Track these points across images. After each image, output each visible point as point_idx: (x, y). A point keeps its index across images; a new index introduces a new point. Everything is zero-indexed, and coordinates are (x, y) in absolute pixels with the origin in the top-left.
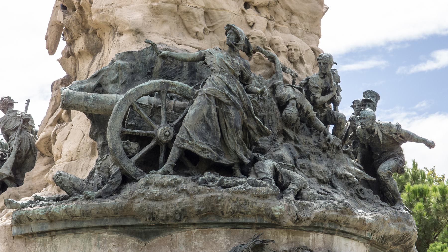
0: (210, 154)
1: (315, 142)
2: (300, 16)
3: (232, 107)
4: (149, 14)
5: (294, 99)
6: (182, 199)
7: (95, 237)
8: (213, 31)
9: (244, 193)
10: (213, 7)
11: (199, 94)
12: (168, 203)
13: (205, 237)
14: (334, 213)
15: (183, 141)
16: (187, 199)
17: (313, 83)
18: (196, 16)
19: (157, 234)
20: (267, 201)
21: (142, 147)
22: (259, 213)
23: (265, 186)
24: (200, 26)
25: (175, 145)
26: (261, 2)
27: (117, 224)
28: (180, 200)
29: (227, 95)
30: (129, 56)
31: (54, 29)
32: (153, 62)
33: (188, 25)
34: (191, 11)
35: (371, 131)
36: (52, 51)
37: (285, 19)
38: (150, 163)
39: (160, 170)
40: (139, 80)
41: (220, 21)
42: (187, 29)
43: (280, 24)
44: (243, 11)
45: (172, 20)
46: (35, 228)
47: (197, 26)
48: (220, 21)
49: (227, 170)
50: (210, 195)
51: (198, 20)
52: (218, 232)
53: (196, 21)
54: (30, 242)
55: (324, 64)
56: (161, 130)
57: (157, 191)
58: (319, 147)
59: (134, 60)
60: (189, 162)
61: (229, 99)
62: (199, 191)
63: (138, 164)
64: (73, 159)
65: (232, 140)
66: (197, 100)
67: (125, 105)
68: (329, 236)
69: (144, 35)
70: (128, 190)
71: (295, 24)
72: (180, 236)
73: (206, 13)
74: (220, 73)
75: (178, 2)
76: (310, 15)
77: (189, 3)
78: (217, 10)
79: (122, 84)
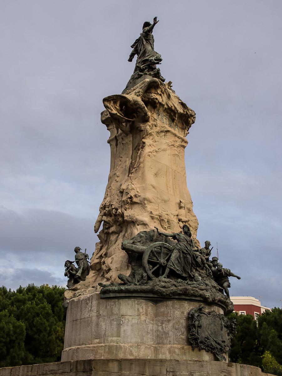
0: (180, 272)
1: (205, 273)
2: (193, 228)
3: (188, 255)
5: (200, 256)
6: (173, 288)
7: (137, 300)
9: (196, 288)
10: (170, 219)
11: (175, 249)
12: (168, 289)
13: (180, 304)
14: (222, 299)
15: (171, 266)
16: (175, 288)
17: (203, 251)
19: (161, 301)
20: (203, 292)
21: (153, 267)
22: (201, 296)
23: (203, 286)
25: (168, 267)
27: (146, 296)
28: (172, 288)
29: (186, 250)
30: (145, 233)
31: (98, 223)
32: (153, 236)
33: (162, 224)
35: (220, 271)
36: (96, 232)
38: (157, 274)
39: (163, 276)
40: (148, 242)
42: (161, 226)
44: (178, 223)
45: (158, 222)
46: (112, 295)
49: (184, 279)
50: (184, 287)
52: (184, 302)
54: (109, 301)
55: (208, 244)
56: (162, 261)
57: (163, 284)
58: (206, 274)
59: (147, 234)
60: (173, 274)
61: (187, 252)
62: (180, 285)
63: (153, 273)
64: (119, 270)
65: (187, 268)
66: (175, 251)
67: (150, 250)
68: (219, 308)
70: (151, 283)
72: (170, 303)
73: (168, 221)
74: (183, 242)
79: (142, 243)
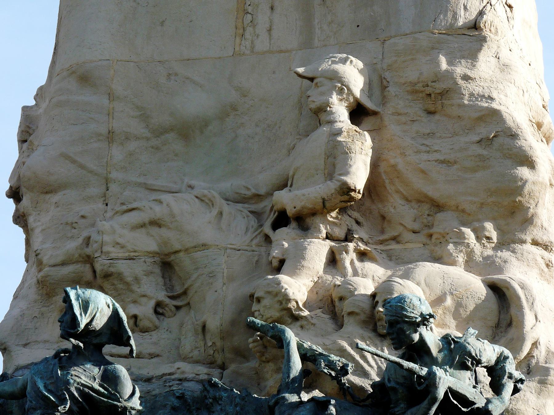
4: (35, 302)
8: (188, 304)
10: (177, 247)
18: (129, 279)
24: (144, 300)
26: (303, 203)
34: (112, 270)
37: (416, 226)
41: (195, 276)
43: (398, 242)
47: (135, 302)
48: (195, 276)
51: (135, 288)
53: (132, 291)
69: (12, 354)
71: (440, 233)
75: (89, 257)
76: (490, 200)
77: (108, 253)
78: (186, 250)
